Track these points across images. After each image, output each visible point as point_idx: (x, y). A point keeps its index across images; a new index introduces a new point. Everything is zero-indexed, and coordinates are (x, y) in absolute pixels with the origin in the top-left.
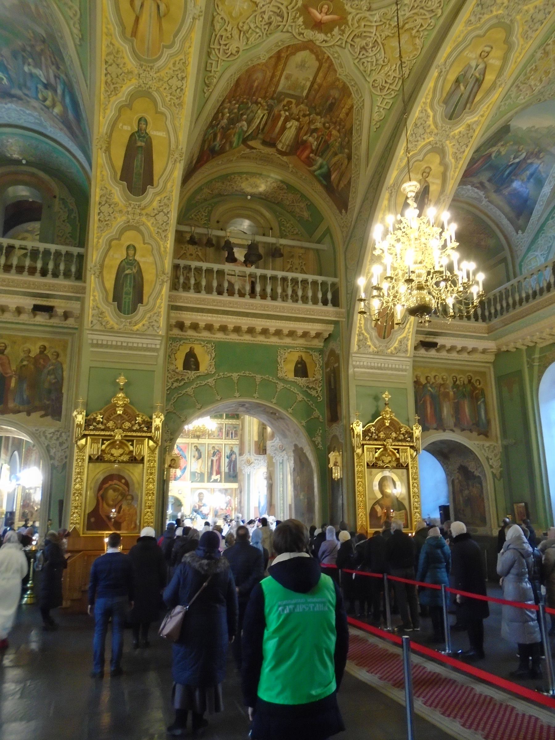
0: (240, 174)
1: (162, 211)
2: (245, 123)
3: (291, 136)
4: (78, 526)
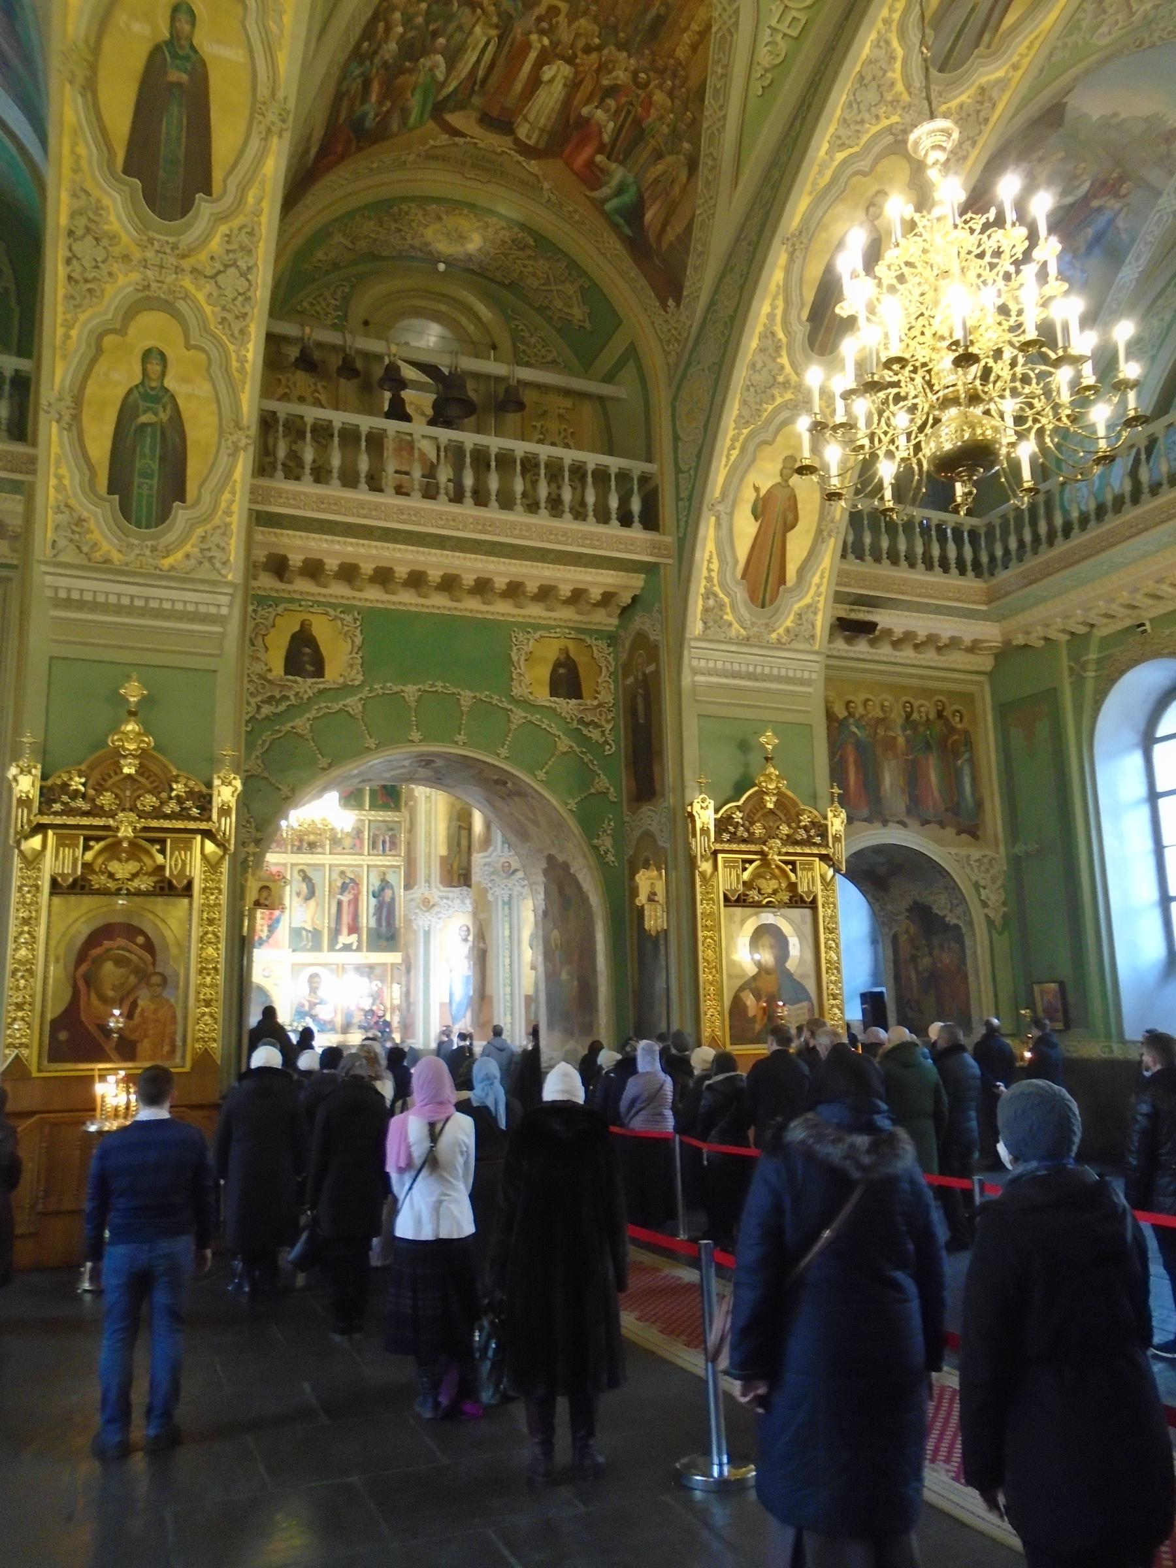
0: (424, 201)
1: (234, 264)
2: (439, 58)
3: (551, 104)
4: (25, 1052)
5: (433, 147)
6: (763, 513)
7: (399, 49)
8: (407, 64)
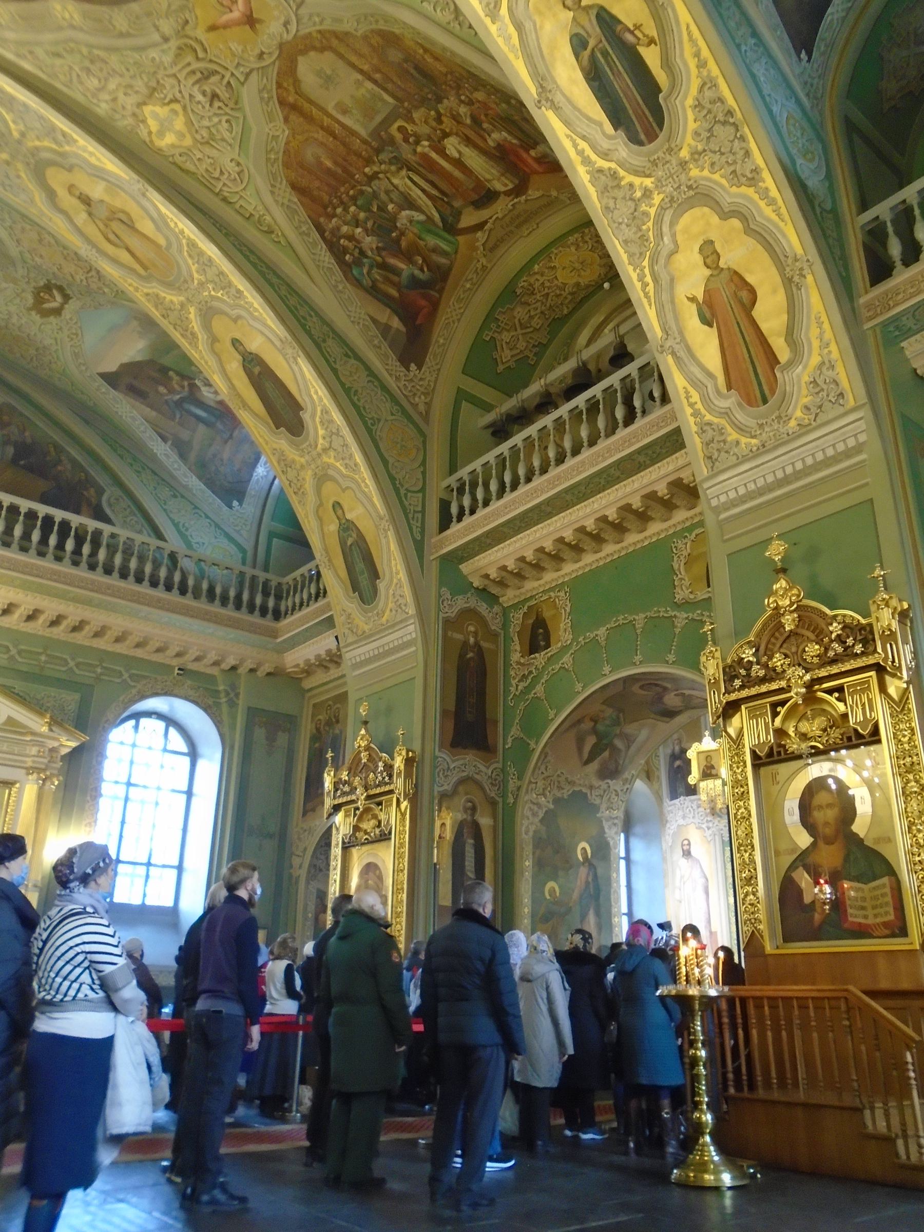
2: (405, 213)
5: (483, 245)
6: (713, 315)
7: (378, 235)
8: (394, 234)
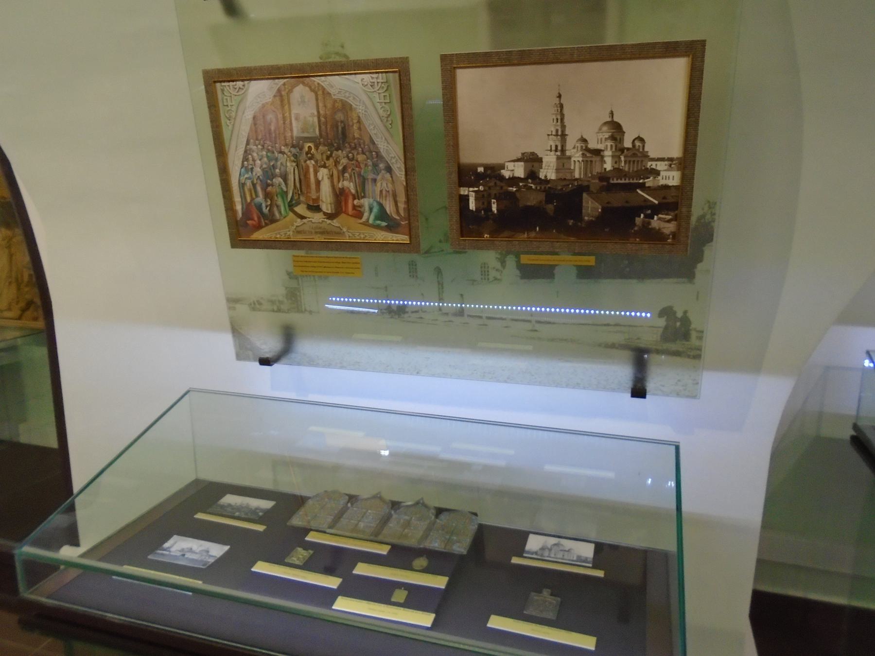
2: (280, 180)
